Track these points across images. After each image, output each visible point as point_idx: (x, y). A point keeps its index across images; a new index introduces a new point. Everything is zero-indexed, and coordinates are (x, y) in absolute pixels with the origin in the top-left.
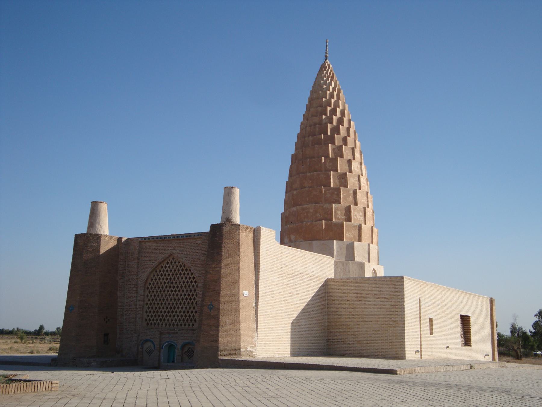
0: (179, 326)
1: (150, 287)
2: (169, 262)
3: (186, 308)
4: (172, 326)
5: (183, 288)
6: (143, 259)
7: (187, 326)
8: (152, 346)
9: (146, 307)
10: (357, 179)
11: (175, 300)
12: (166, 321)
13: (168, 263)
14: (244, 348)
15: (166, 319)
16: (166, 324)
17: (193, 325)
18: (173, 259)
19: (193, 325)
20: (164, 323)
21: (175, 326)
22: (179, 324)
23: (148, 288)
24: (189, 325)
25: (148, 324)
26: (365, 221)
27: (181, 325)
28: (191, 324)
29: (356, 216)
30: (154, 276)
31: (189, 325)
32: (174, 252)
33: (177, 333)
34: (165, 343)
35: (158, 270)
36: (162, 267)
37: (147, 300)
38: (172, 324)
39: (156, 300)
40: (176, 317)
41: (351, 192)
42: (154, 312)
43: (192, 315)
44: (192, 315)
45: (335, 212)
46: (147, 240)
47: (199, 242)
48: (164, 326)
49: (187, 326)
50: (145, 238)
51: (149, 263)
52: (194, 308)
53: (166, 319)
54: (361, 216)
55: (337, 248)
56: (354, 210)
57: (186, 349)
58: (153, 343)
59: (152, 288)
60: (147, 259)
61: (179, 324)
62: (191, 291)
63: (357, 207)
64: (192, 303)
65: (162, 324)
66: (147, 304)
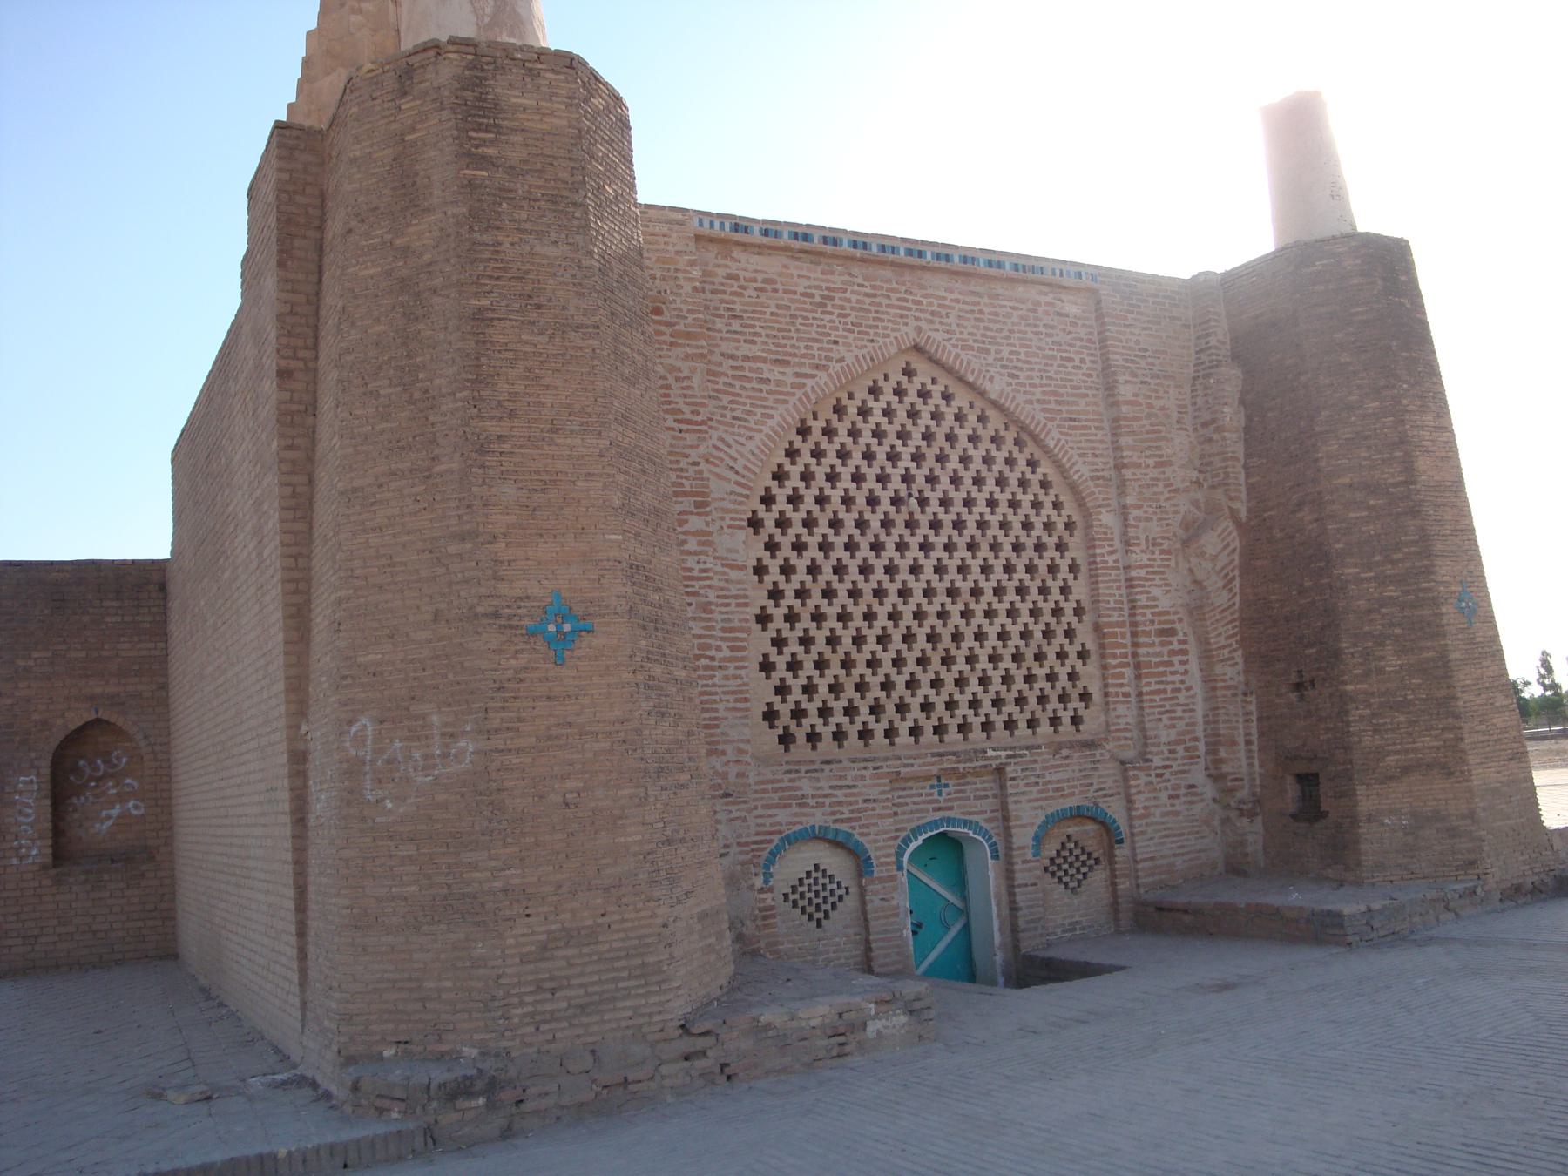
0: (999, 733)
1: (769, 519)
2: (888, 388)
3: (1025, 635)
4: (953, 735)
5: (994, 531)
6: (725, 347)
7: (1045, 728)
8: (836, 863)
9: (760, 642)
11: (952, 592)
12: (915, 713)
13: (875, 391)
15: (915, 702)
16: (915, 731)
17: (1076, 720)
18: (908, 372)
19: (1076, 720)
20: (903, 727)
21: (977, 735)
22: (998, 720)
23: (755, 524)
24: (1055, 721)
25: (786, 739)
27: (1010, 725)
28: (1066, 717)
30: (792, 454)
31: (1055, 721)
32: (938, 336)
33: (1000, 770)
34: (916, 832)
35: (817, 426)
36: (839, 410)
37: (760, 598)
38: (952, 724)
39: (829, 594)
40: (974, 686)
42: (821, 665)
43: (1063, 672)
44: (1063, 672)
46: (785, 238)
47: (1072, 309)
48: (903, 738)
49: (1045, 728)
50: (740, 225)
51: (772, 372)
52: (1069, 633)
53: (915, 702)
57: (1051, 849)
58: (839, 843)
59: (782, 523)
60: (755, 350)
61: (998, 720)
62: (1040, 547)
64: (1057, 612)
65: (890, 733)
66: (763, 619)
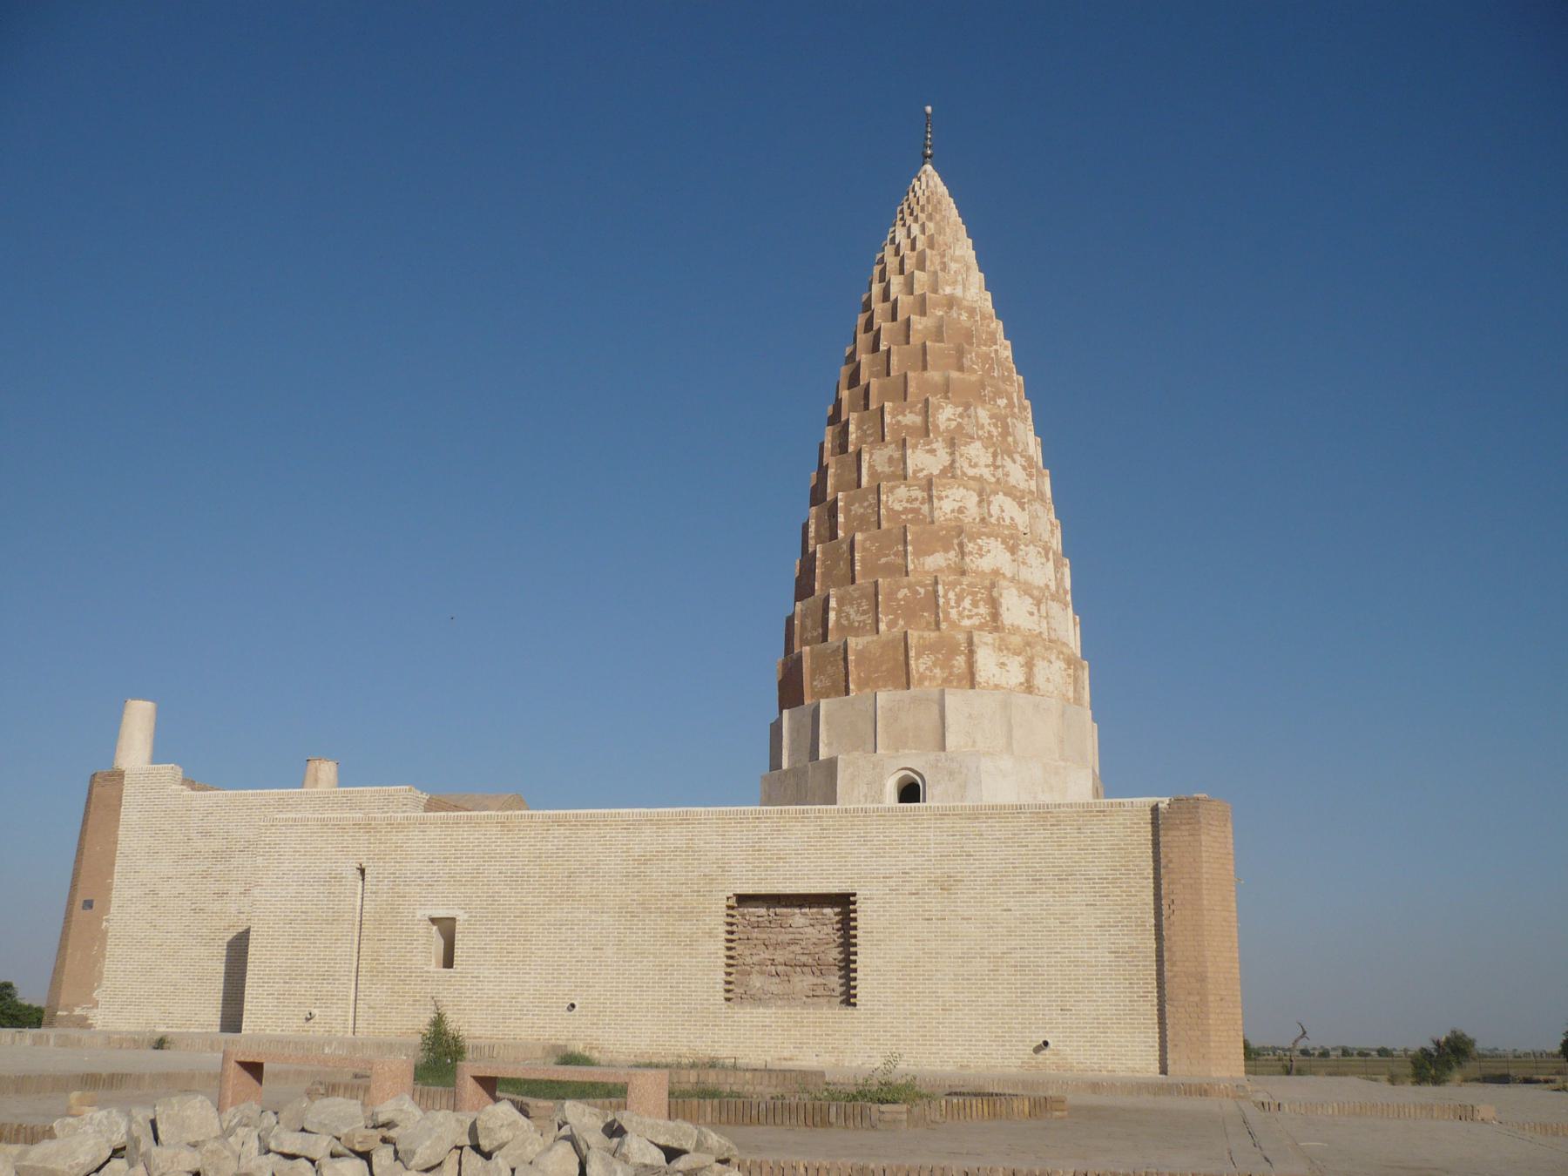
10: (872, 498)
14: (67, 1008)
26: (877, 621)
29: (848, 617)
41: (845, 547)
45: (802, 624)
54: (864, 612)
55: (792, 730)
56: (841, 602)
63: (852, 588)
